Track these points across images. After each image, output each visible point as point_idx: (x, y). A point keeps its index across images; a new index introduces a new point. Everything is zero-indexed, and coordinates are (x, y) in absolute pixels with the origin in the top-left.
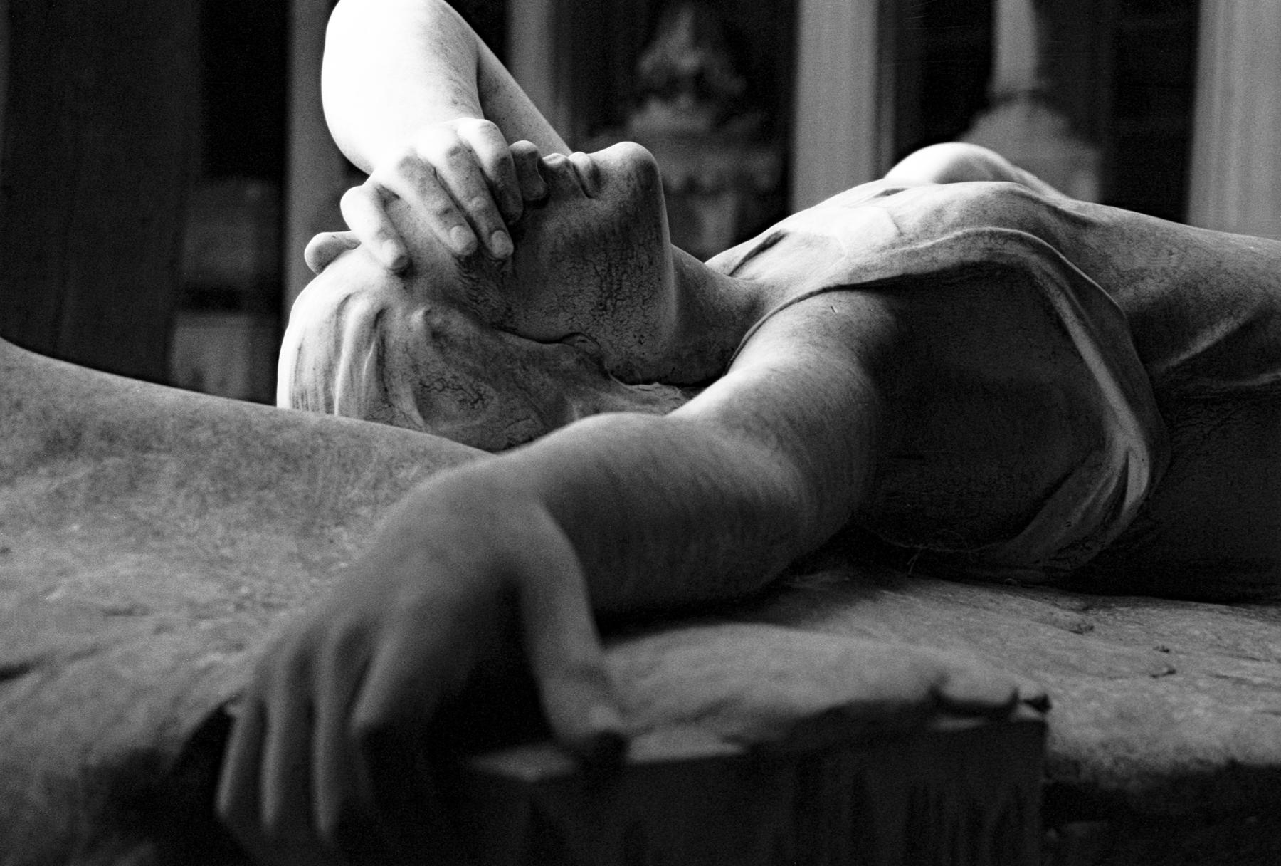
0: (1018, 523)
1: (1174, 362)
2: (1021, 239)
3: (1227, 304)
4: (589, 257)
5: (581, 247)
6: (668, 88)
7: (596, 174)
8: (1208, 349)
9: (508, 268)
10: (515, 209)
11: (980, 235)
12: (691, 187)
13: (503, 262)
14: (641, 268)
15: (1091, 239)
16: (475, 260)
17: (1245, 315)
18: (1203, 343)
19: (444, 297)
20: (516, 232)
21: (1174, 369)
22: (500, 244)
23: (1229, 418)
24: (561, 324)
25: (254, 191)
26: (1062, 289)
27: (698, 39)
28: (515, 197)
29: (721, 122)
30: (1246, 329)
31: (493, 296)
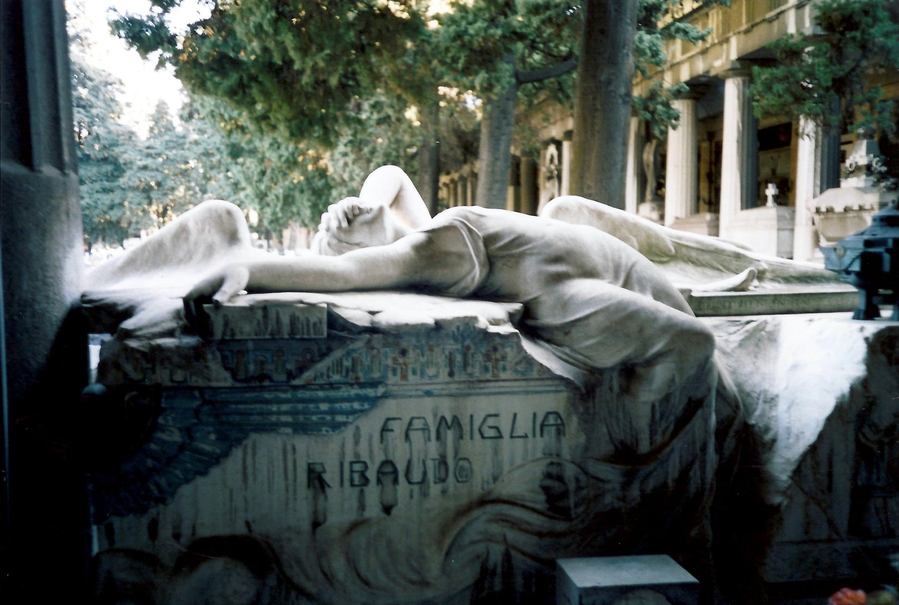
0: (455, 283)
3: (510, 233)
6: (856, 170)
7: (371, 209)
10: (350, 217)
12: (861, 208)
15: (482, 220)
16: (340, 228)
18: (501, 243)
19: (334, 236)
20: (350, 222)
22: (345, 224)
25: (708, 216)
27: (868, 153)
29: (875, 184)
31: (343, 236)
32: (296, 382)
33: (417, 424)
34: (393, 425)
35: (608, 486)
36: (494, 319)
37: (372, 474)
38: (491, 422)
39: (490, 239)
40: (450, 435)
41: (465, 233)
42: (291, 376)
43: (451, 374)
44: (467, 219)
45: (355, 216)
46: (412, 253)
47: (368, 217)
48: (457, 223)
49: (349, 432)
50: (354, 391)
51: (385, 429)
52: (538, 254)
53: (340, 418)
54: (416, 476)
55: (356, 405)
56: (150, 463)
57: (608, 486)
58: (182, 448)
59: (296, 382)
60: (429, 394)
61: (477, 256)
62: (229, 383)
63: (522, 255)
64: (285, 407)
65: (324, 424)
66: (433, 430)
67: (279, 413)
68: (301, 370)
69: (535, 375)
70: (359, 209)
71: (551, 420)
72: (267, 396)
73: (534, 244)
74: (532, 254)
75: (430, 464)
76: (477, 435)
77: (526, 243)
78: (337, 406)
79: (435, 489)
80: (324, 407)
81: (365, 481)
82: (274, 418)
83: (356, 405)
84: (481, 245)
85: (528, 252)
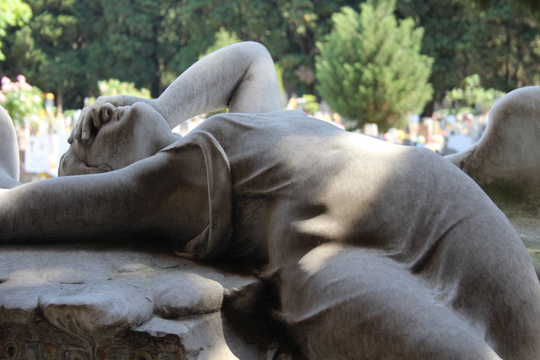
1: (242, 182)
2: (204, 135)
4: (107, 140)
5: (105, 137)
7: (122, 113)
8: (254, 178)
9: (89, 144)
10: (95, 125)
11: (195, 133)
13: (87, 141)
14: (124, 144)
17: (272, 165)
21: (242, 185)
22: (84, 136)
23: (261, 205)
24: (99, 161)
26: (206, 153)
28: (96, 121)
30: (270, 171)
31: (82, 152)
36: (169, 308)
39: (238, 170)
41: (208, 158)
44: (217, 133)
45: (103, 122)
46: (134, 184)
48: (201, 142)
52: (291, 198)
61: (213, 194)
63: (271, 200)
70: (110, 112)
73: (294, 180)
74: (285, 197)
77: (287, 177)
84: (223, 176)
85: (280, 193)
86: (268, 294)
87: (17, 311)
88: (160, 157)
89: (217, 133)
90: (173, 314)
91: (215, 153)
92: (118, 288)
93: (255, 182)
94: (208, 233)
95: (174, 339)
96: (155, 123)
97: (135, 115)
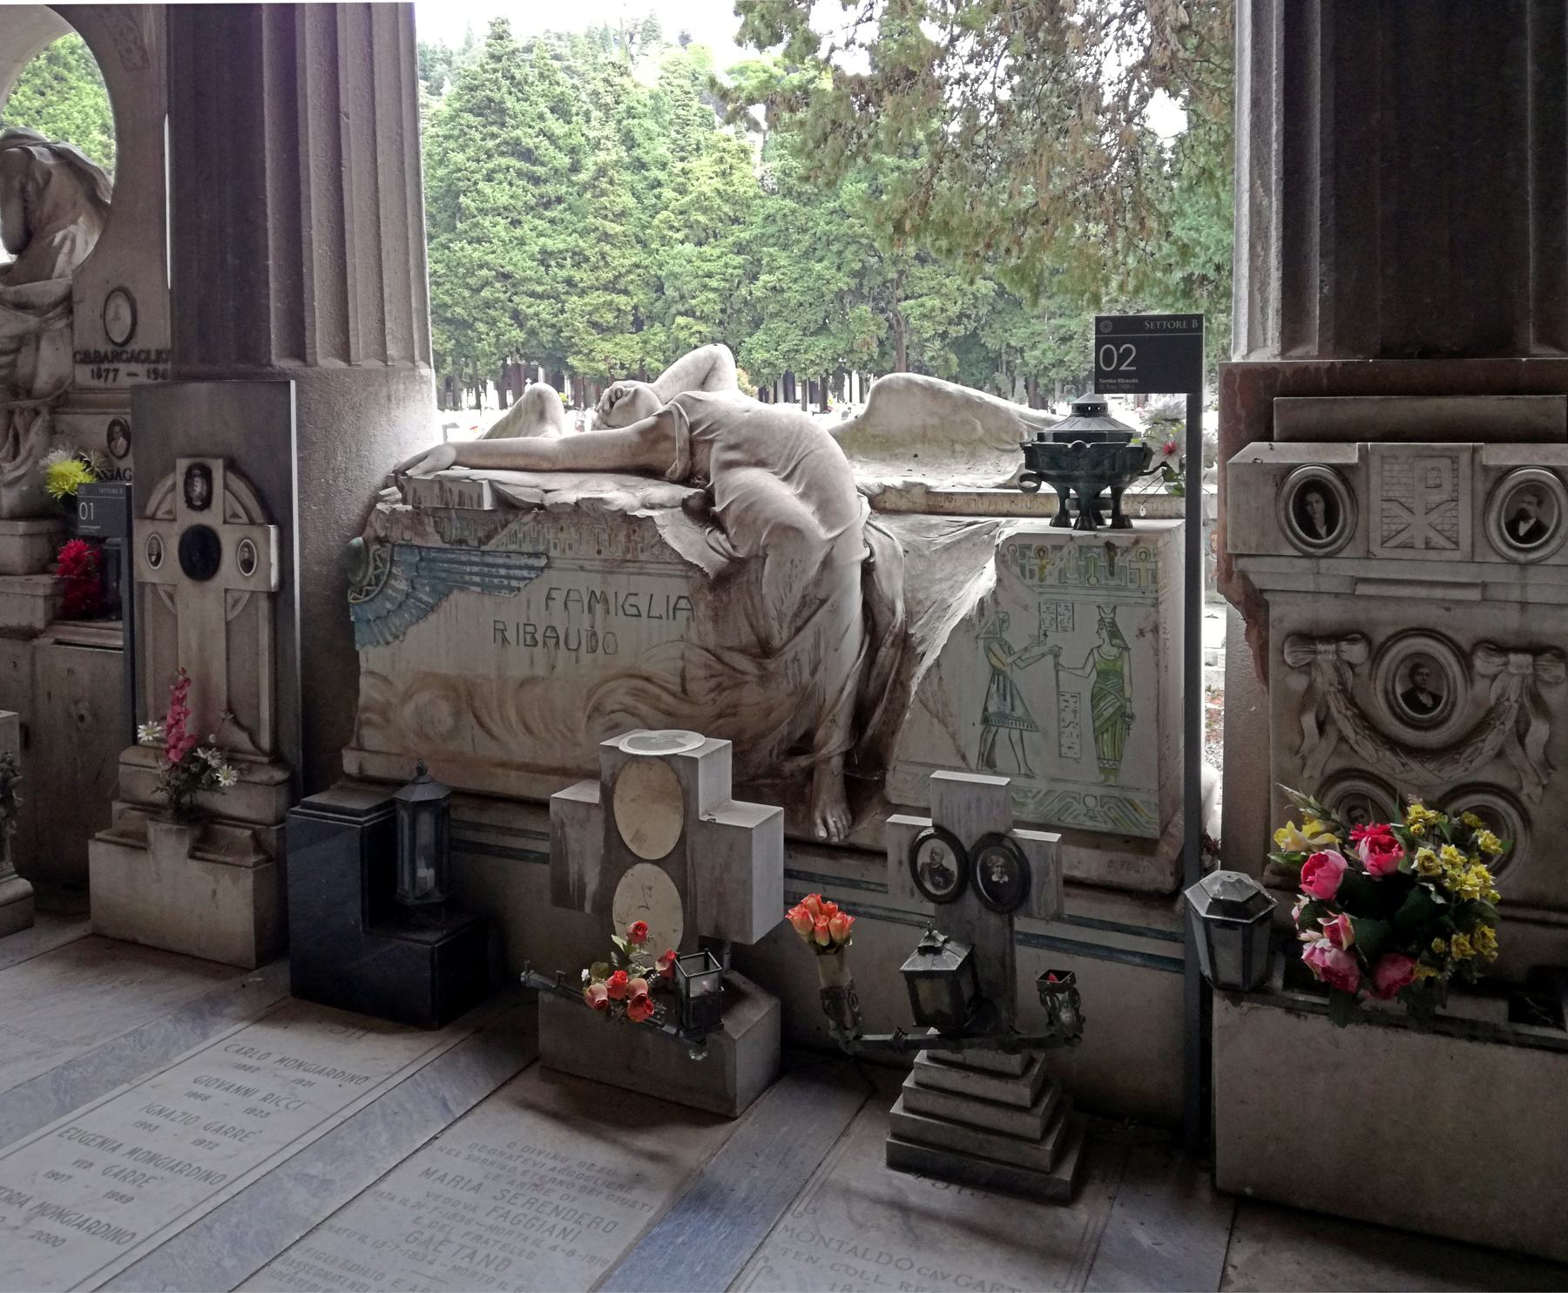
20: (612, 404)
32: (484, 548)
33: (573, 596)
34: (554, 594)
35: (748, 678)
37: (539, 637)
38: (632, 600)
40: (599, 608)
42: (481, 542)
43: (599, 552)
47: (625, 399)
49: (523, 595)
50: (524, 561)
51: (549, 598)
53: (514, 583)
54: (573, 645)
55: (525, 573)
56: (389, 606)
57: (748, 678)
58: (408, 596)
59: (484, 548)
60: (582, 568)
62: (440, 544)
64: (476, 569)
65: (500, 587)
66: (586, 601)
67: (471, 574)
68: (489, 537)
69: (667, 557)
71: (683, 603)
72: (464, 558)
75: (584, 634)
76: (620, 611)
78: (512, 572)
79: (586, 657)
80: (503, 572)
81: (535, 644)
82: (467, 578)
83: (525, 573)
84: (685, 431)
86: (709, 498)
87: (565, 504)
88: (651, 420)
89: (683, 403)
90: (652, 507)
91: (681, 415)
92: (619, 494)
93: (703, 433)
94: (678, 466)
95: (650, 518)
96: (648, 398)
97: (636, 392)
